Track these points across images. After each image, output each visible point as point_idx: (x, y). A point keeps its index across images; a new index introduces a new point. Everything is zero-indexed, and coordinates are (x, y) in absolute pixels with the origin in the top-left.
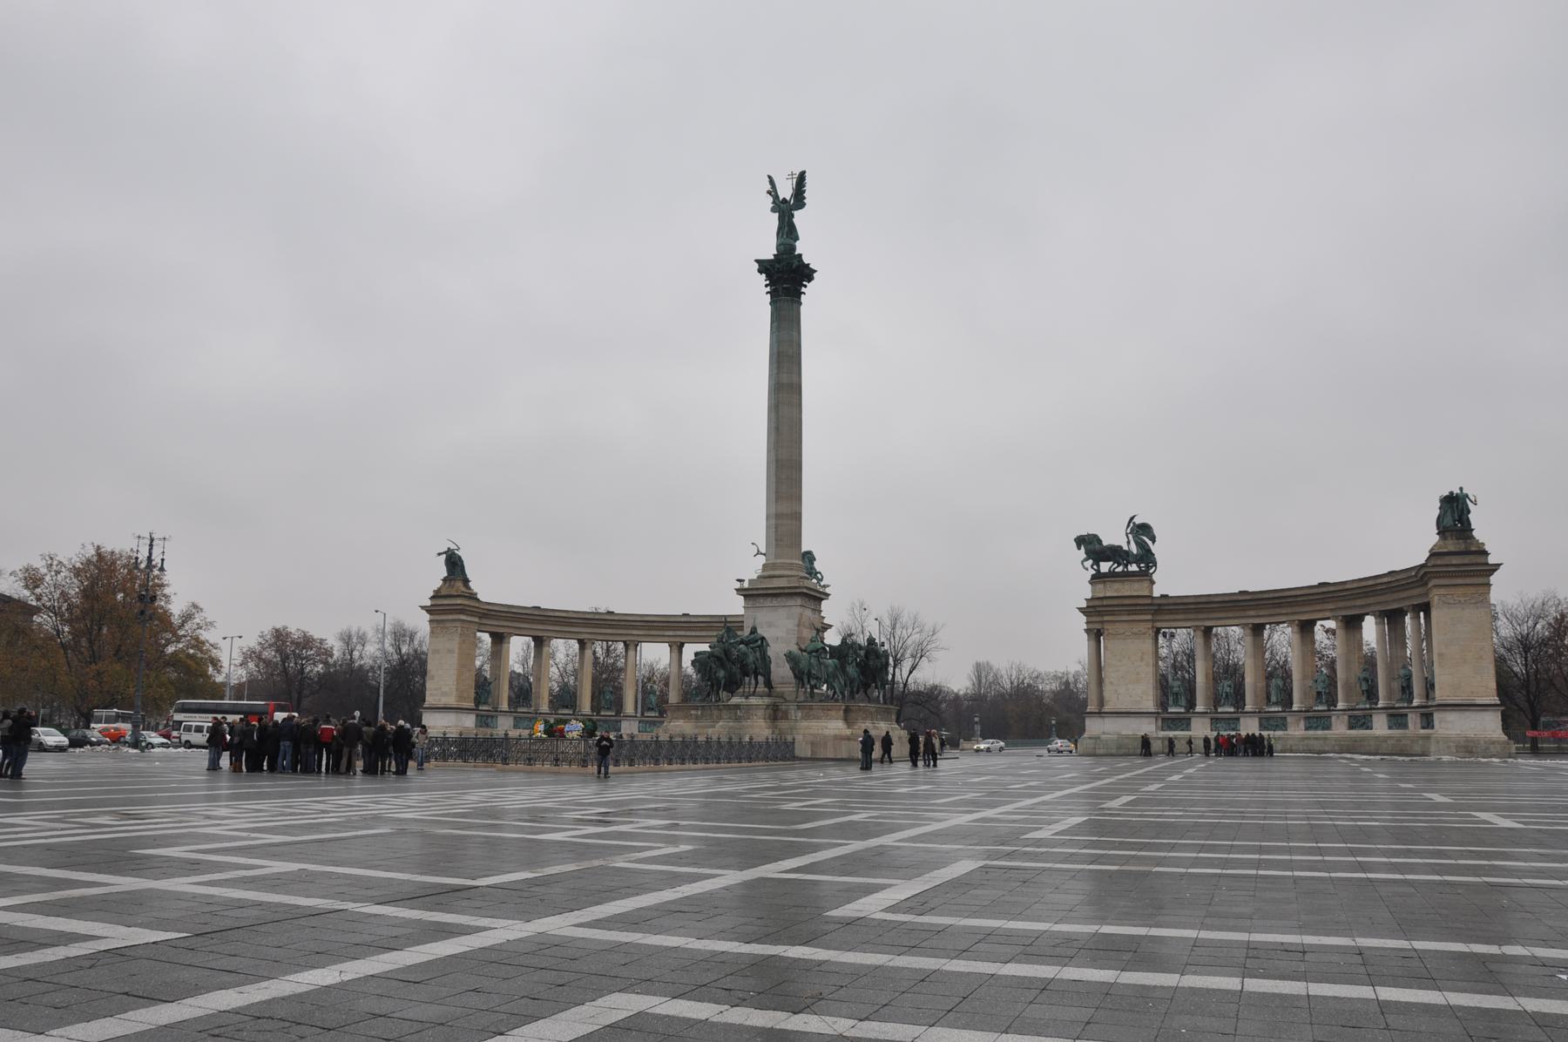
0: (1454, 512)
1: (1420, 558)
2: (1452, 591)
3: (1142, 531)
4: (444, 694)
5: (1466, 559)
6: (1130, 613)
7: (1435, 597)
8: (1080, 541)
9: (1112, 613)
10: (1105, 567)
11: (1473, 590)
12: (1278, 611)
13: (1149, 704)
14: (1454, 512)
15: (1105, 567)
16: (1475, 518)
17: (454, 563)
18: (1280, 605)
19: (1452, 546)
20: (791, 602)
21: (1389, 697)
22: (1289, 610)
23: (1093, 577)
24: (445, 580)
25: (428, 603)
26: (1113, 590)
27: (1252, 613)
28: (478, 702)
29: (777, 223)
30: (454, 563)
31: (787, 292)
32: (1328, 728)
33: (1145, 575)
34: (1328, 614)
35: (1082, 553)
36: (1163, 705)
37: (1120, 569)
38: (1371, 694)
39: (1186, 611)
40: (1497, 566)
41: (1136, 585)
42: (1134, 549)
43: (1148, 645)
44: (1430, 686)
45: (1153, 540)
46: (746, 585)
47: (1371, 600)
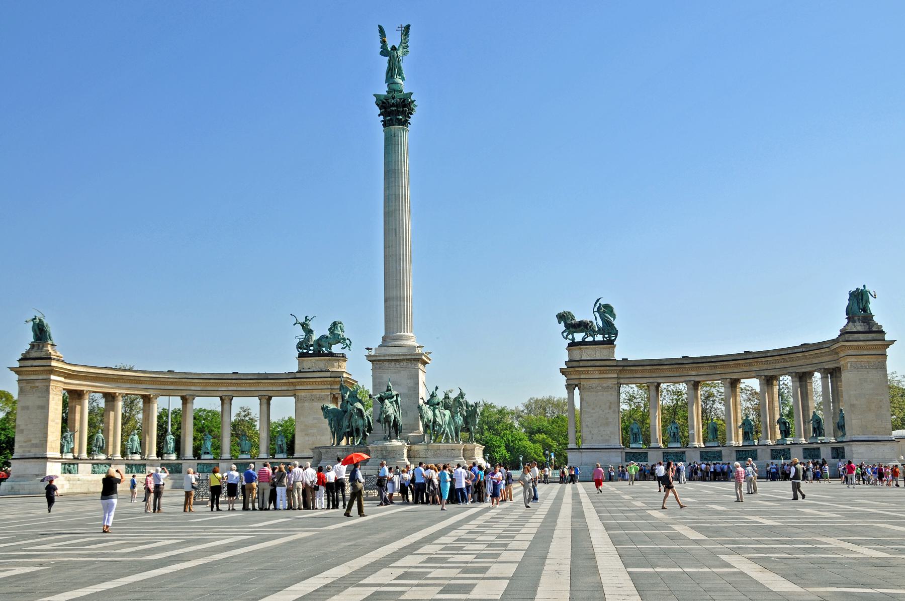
0: (859, 302)
1: (835, 335)
3: (605, 311)
4: (36, 446)
5: (870, 336)
6: (601, 372)
7: (847, 362)
8: (562, 317)
9: (587, 372)
10: (579, 337)
12: (713, 371)
13: (617, 442)
14: (859, 302)
15: (579, 337)
16: (874, 306)
17: (41, 333)
19: (859, 327)
23: (570, 345)
24: (33, 345)
25: (17, 365)
26: (587, 354)
28: (62, 452)
30: (41, 333)
33: (611, 343)
34: (753, 374)
35: (562, 326)
36: (625, 441)
37: (590, 339)
40: (892, 342)
42: (601, 324)
43: (616, 393)
44: (841, 427)
45: (614, 318)
46: (373, 353)
47: (789, 364)
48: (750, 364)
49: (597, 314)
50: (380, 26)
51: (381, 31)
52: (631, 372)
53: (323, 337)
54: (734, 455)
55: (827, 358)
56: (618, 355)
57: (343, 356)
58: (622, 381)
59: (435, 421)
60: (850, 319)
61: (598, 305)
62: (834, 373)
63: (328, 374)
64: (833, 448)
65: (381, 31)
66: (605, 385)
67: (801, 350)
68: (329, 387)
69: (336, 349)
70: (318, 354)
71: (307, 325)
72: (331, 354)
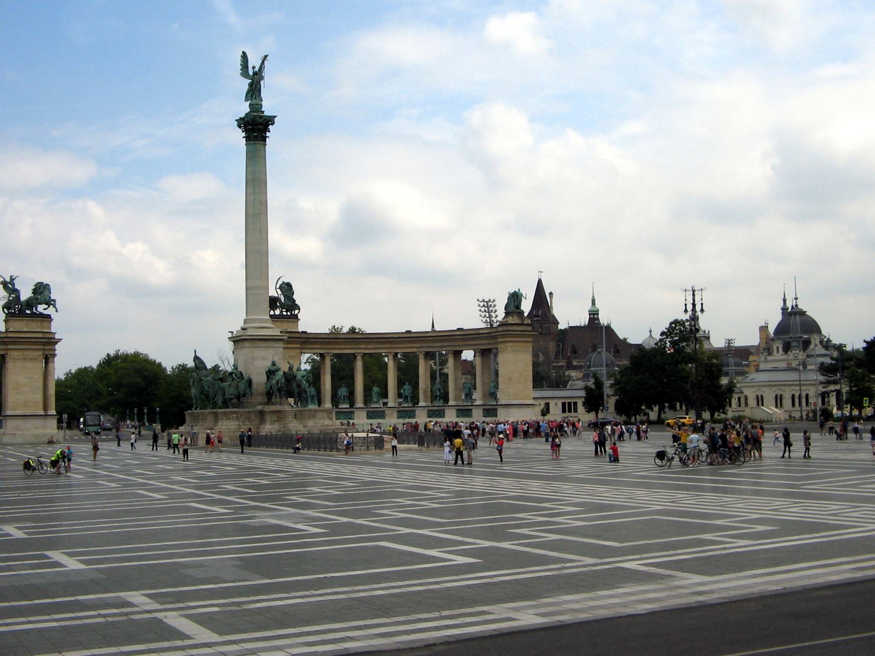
2: (516, 344)
3: (287, 288)
11: (524, 344)
12: (380, 346)
18: (382, 343)
20: (276, 345)
21: (457, 398)
22: (388, 346)
27: (363, 346)
29: (246, 88)
31: (256, 139)
32: (414, 417)
33: (296, 317)
38: (445, 398)
39: (322, 343)
41: (291, 325)
44: (493, 395)
48: (413, 342)
49: (280, 292)
50: (244, 53)
51: (244, 56)
52: (312, 343)
53: (30, 299)
54: (395, 414)
55: (484, 342)
56: (300, 330)
57: (49, 316)
58: (304, 351)
59: (305, 391)
60: (507, 314)
61: (280, 282)
62: (485, 353)
63: (40, 335)
64: (484, 410)
65: (244, 56)
66: (290, 354)
67: (458, 333)
68: (42, 347)
69: (41, 308)
70: (21, 314)
71: (13, 285)
72: (41, 315)
